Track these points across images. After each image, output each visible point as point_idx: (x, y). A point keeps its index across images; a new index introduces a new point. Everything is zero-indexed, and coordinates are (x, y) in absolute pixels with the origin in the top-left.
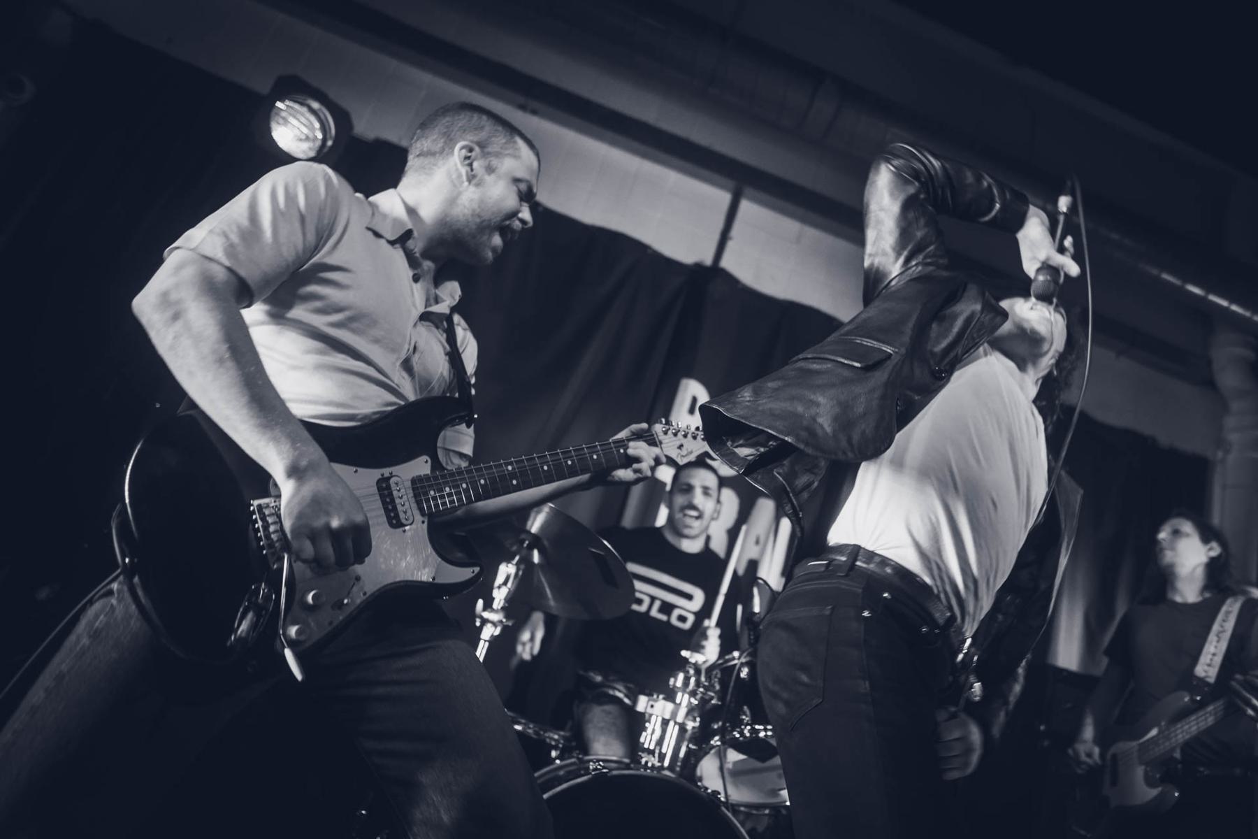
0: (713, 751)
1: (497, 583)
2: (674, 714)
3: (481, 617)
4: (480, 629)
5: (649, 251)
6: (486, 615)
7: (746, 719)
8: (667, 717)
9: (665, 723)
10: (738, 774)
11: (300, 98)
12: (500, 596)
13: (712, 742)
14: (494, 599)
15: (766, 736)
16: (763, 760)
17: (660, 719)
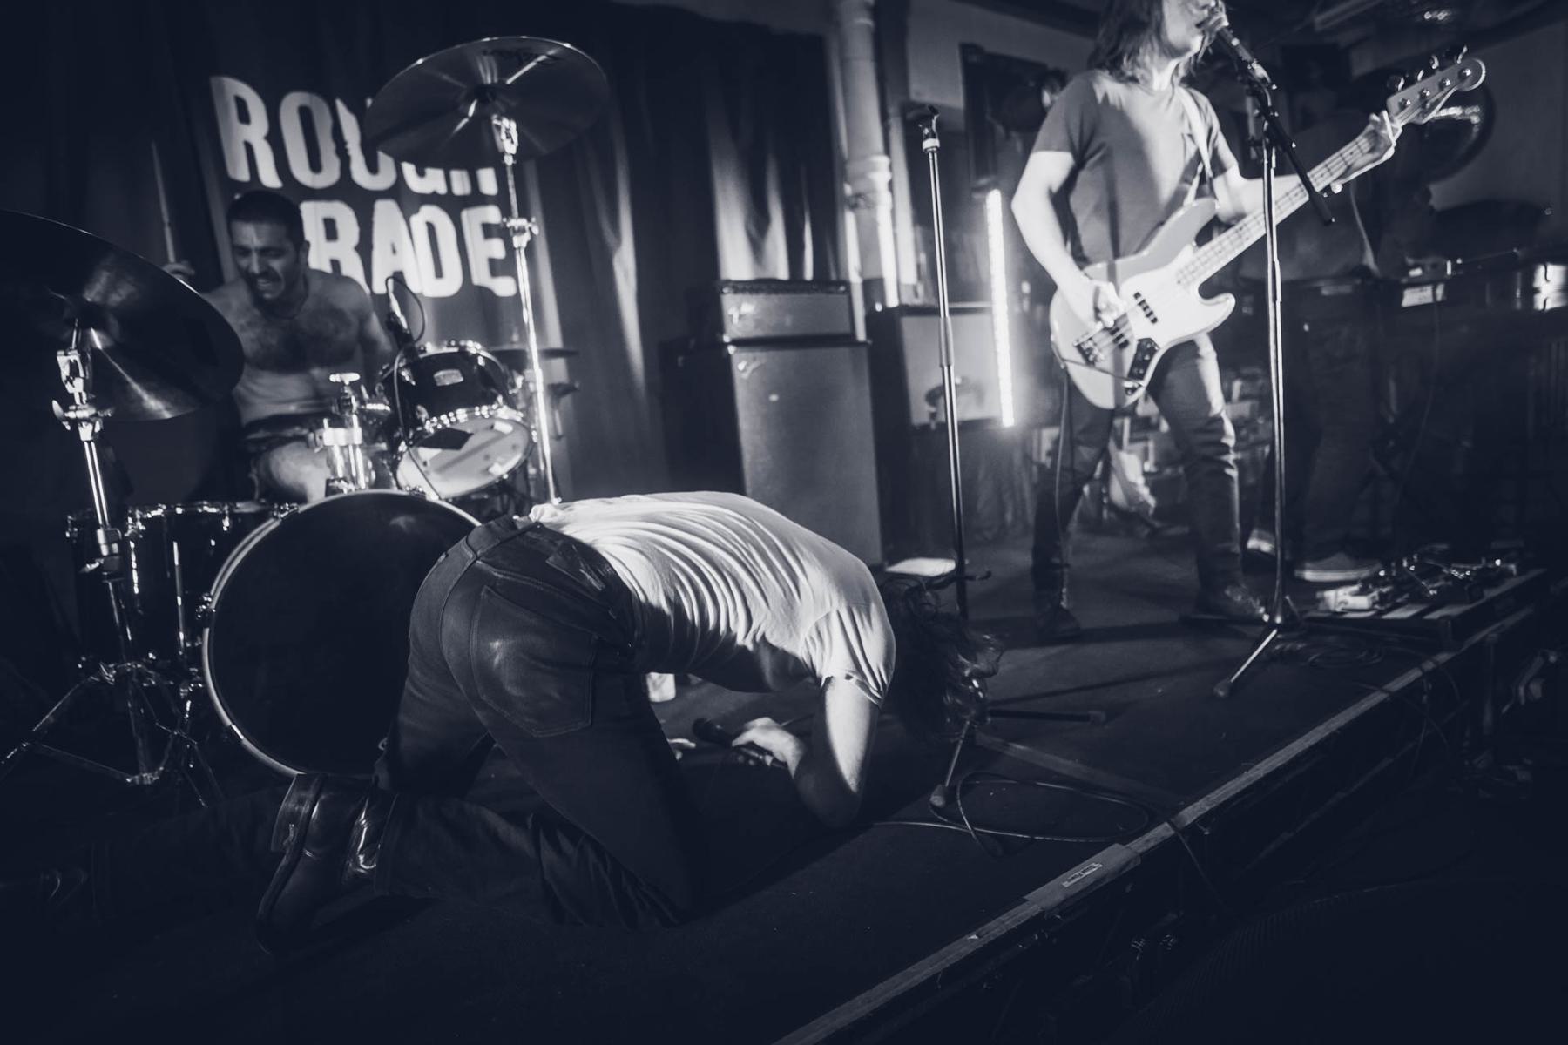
0: (405, 456)
2: (350, 438)
8: (344, 444)
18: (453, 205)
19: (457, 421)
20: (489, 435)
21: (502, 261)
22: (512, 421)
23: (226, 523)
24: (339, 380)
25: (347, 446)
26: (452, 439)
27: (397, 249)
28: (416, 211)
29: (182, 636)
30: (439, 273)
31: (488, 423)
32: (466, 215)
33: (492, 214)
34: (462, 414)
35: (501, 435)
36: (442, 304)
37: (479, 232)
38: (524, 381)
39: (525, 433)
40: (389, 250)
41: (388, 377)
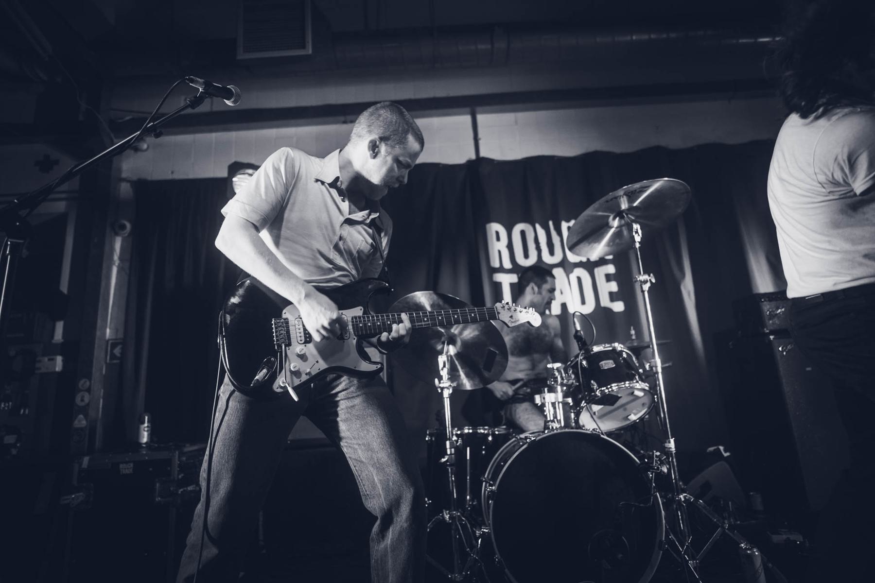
0: (584, 409)
1: (440, 368)
2: (557, 398)
3: (440, 387)
4: (442, 393)
5: (441, 166)
6: (441, 385)
7: (595, 387)
8: (553, 401)
9: (553, 404)
10: (603, 416)
11: (242, 172)
12: (444, 373)
13: (582, 405)
14: (442, 376)
15: (609, 391)
16: (612, 404)
17: (550, 405)
18: (590, 266)
19: (612, 390)
20: (631, 398)
21: (616, 293)
22: (643, 390)
23: (490, 438)
24: (551, 367)
25: (555, 402)
26: (609, 400)
27: (563, 292)
28: (572, 272)
29: (468, 497)
30: (583, 302)
31: (631, 391)
32: (596, 270)
33: (611, 269)
34: (614, 387)
35: (637, 397)
36: (584, 318)
37: (604, 279)
38: (650, 366)
39: (650, 397)
40: (560, 293)
41: (575, 363)
